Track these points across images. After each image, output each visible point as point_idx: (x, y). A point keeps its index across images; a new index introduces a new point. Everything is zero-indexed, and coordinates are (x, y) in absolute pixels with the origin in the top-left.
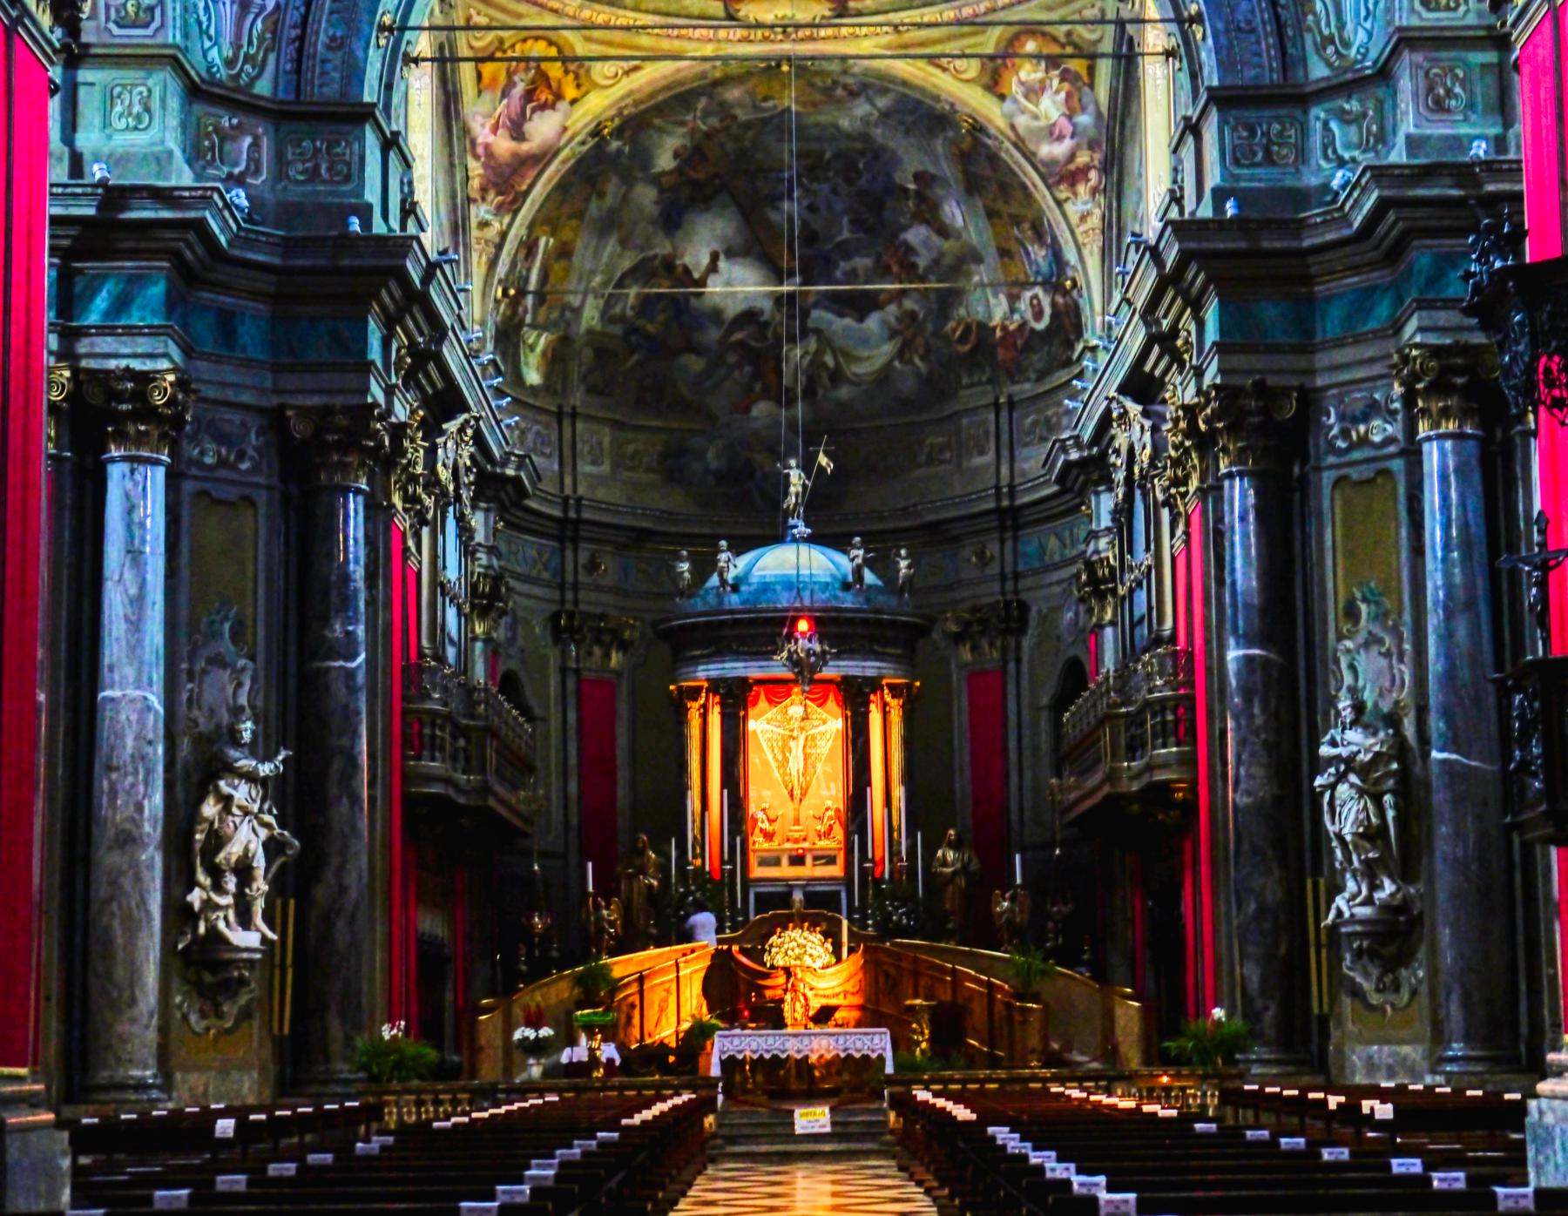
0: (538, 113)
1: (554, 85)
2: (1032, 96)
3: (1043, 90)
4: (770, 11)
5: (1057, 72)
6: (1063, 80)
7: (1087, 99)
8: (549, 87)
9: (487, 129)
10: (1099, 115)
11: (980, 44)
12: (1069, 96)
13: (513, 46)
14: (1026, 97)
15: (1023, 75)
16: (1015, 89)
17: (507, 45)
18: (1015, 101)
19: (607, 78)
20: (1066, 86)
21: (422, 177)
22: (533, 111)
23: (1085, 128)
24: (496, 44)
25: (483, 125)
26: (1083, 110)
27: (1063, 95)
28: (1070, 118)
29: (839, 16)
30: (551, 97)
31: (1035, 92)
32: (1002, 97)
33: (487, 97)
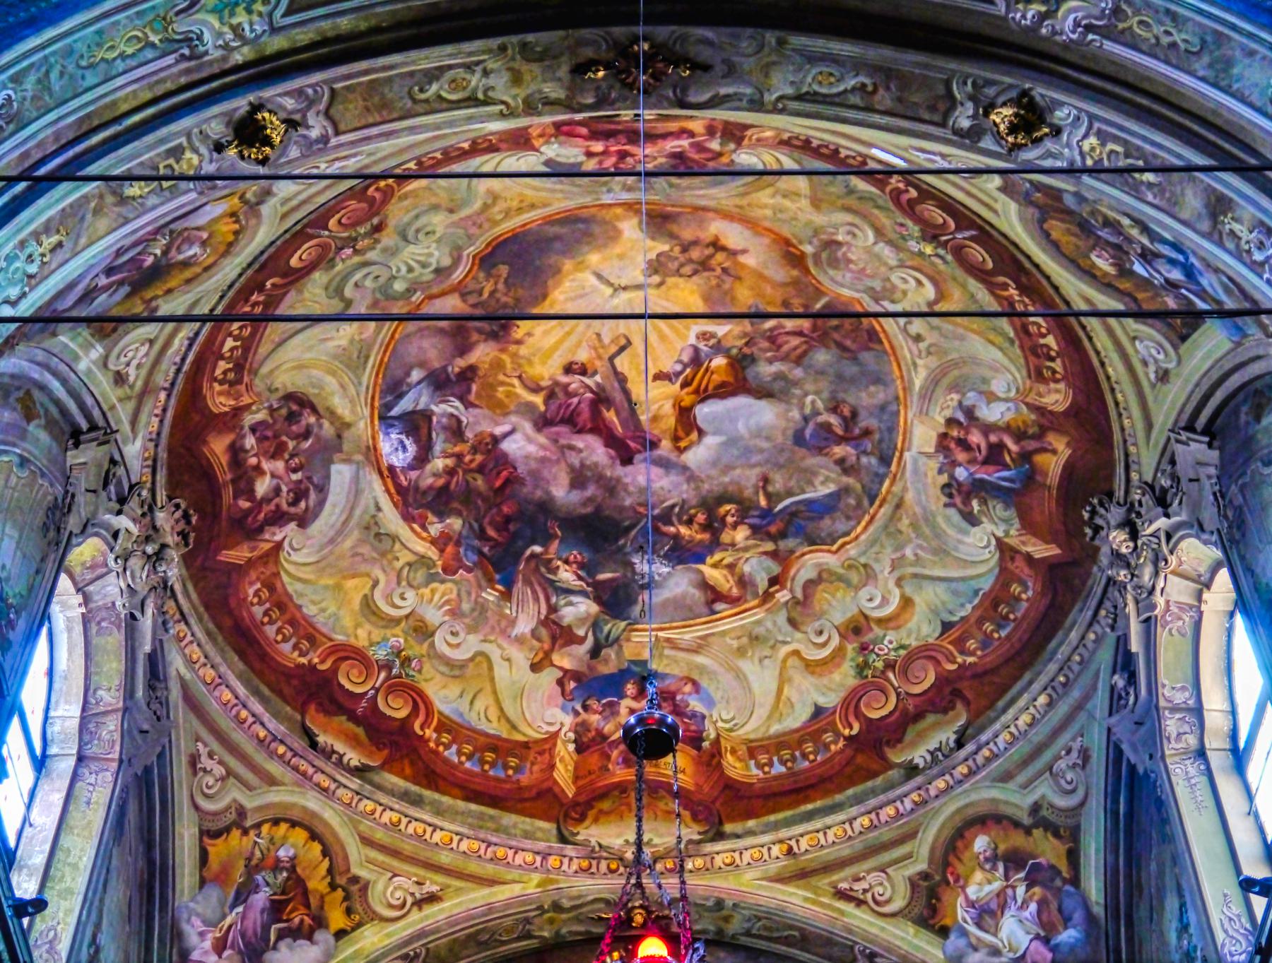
0: (289, 940)
1: (314, 902)
2: (988, 920)
3: (1003, 907)
4: (619, 836)
5: (1022, 875)
6: (1031, 882)
7: (1069, 904)
8: (308, 906)
9: (208, 944)
10: (1090, 918)
11: (909, 856)
12: (1042, 903)
13: (258, 826)
14: (979, 925)
15: (972, 891)
16: (962, 913)
17: (248, 823)
18: (964, 933)
19: (391, 906)
20: (1037, 890)
21: (69, 891)
22: (280, 937)
23: (1072, 948)
24: (232, 816)
25: (202, 935)
26: (1067, 921)
27: (1033, 907)
28: (1046, 941)
29: (713, 840)
30: (307, 920)
31: (992, 914)
32: (944, 932)
33: (213, 893)
